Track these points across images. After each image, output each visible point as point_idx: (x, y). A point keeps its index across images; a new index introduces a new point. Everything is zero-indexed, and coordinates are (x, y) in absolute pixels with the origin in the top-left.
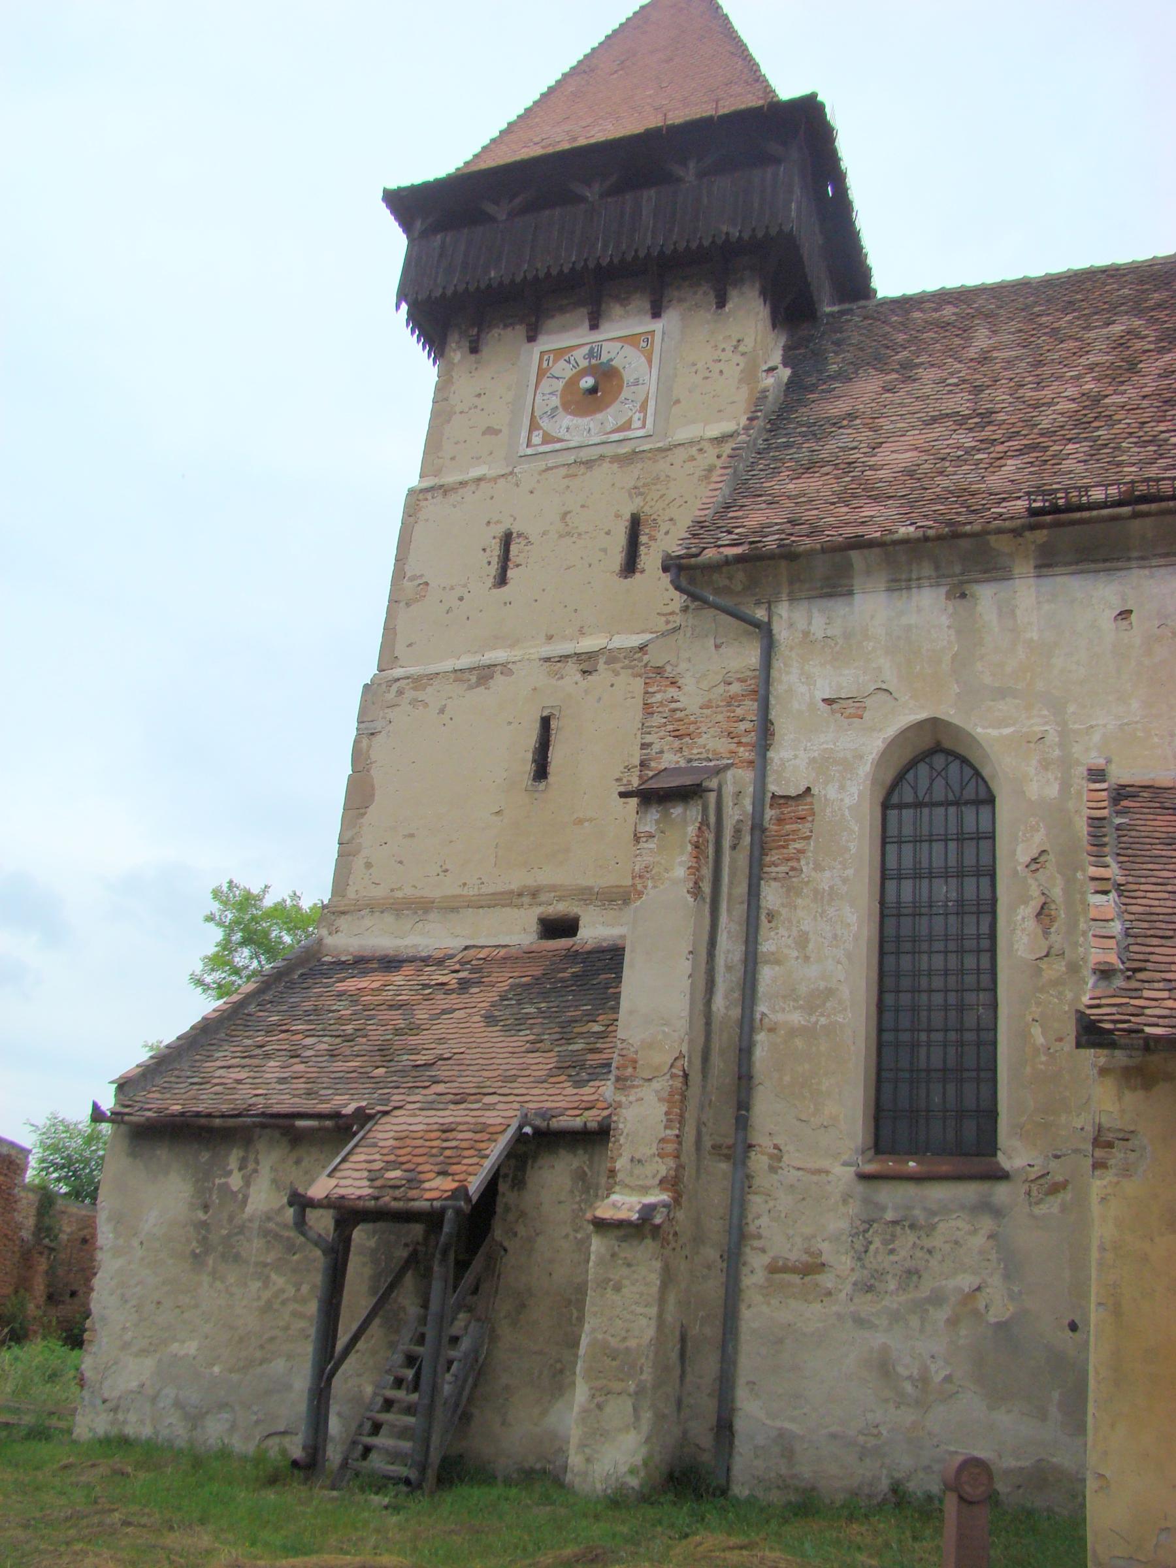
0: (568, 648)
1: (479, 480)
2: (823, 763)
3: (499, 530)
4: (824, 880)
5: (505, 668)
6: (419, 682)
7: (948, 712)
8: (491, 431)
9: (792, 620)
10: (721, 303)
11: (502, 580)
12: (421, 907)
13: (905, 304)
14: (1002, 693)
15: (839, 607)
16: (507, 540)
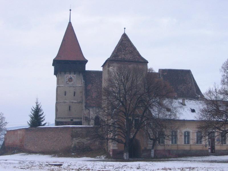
1: (62, 86)
3: (65, 91)
5: (67, 102)
6: (60, 102)
8: (62, 82)
10: (79, 74)
11: (65, 95)
16: (65, 92)
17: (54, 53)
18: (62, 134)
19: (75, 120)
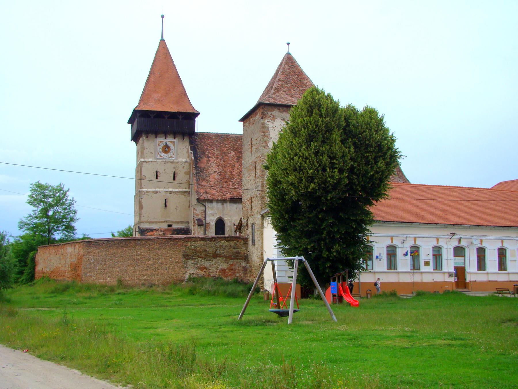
0: (167, 190)
2: (211, 220)
4: (211, 231)
5: (160, 192)
6: (148, 192)
7: (221, 216)
8: (151, 153)
9: (208, 205)
12: (152, 222)
13: (203, 135)
14: (226, 215)
15: (212, 204)
16: (157, 172)
17: (132, 101)
18: (164, 251)
19: (175, 226)
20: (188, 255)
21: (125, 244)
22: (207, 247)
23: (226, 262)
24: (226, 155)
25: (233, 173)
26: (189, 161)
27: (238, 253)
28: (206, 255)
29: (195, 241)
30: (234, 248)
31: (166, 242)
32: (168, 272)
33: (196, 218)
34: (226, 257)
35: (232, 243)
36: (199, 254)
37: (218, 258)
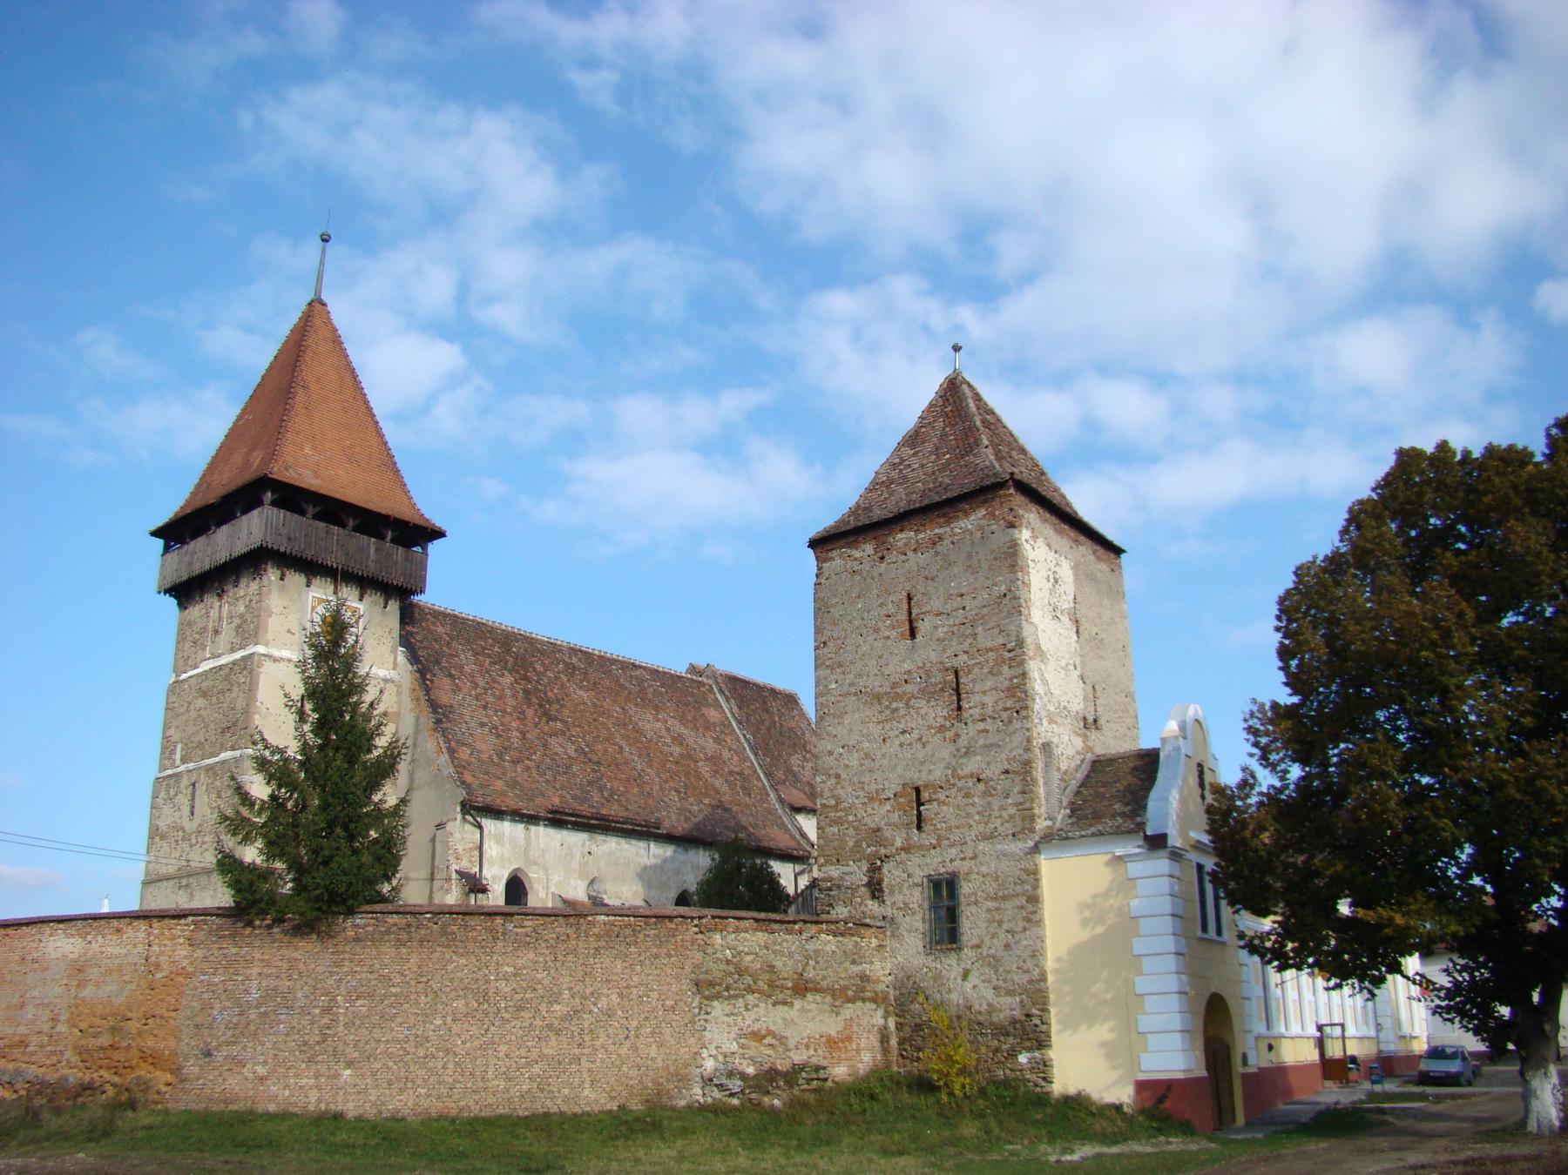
9: (489, 824)
14: (535, 864)
18: (619, 965)
20: (711, 984)
21: (444, 932)
22: (775, 952)
23: (835, 1010)
24: (495, 681)
25: (529, 736)
26: (392, 674)
27: (864, 978)
28: (771, 984)
29: (737, 930)
30: (854, 962)
31: (628, 931)
32: (635, 1048)
33: (454, 867)
34: (833, 992)
35: (849, 942)
36: (749, 980)
37: (809, 997)
